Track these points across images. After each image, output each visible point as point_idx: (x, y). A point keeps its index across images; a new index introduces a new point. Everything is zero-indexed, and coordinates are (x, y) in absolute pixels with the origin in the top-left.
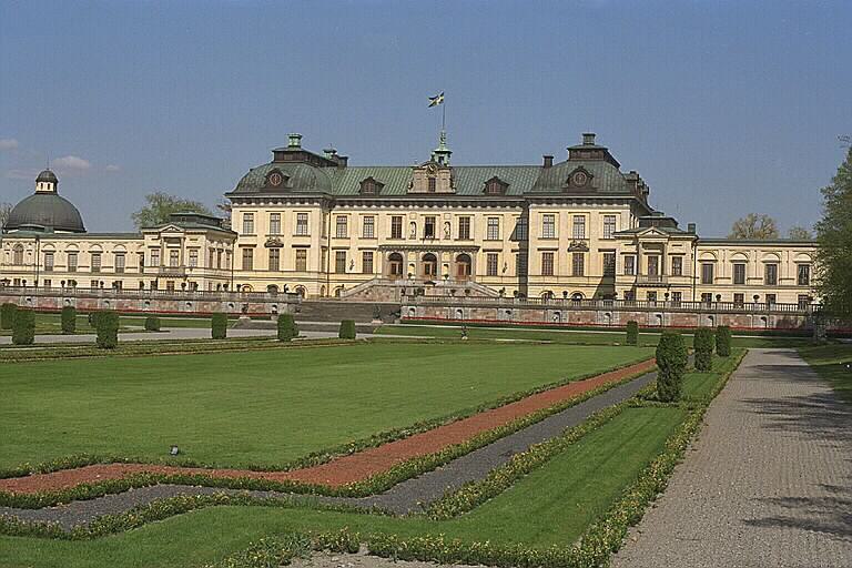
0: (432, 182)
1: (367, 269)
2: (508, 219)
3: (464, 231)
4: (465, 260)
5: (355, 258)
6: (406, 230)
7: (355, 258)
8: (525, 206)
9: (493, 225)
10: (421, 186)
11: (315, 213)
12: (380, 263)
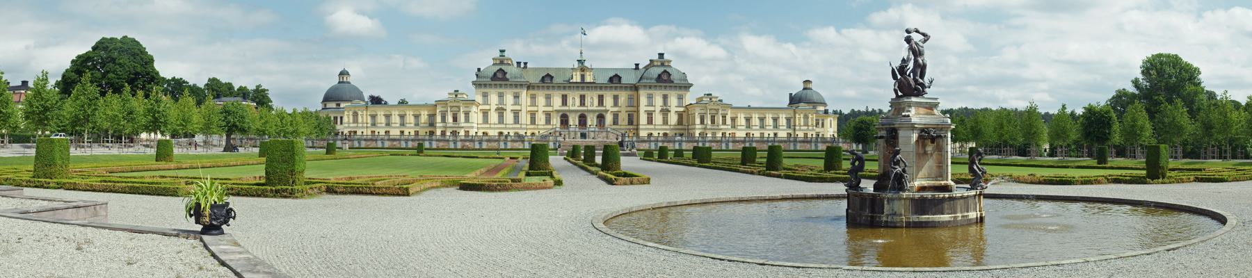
0: (583, 77)
1: (548, 121)
2: (623, 97)
3: (601, 102)
4: (601, 117)
5: (541, 119)
6: (570, 101)
7: (541, 119)
8: (636, 88)
9: (616, 98)
10: (577, 78)
11: (524, 94)
12: (556, 121)
